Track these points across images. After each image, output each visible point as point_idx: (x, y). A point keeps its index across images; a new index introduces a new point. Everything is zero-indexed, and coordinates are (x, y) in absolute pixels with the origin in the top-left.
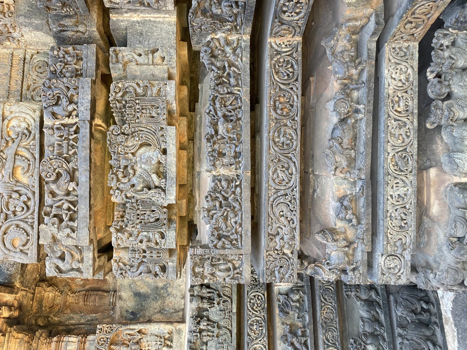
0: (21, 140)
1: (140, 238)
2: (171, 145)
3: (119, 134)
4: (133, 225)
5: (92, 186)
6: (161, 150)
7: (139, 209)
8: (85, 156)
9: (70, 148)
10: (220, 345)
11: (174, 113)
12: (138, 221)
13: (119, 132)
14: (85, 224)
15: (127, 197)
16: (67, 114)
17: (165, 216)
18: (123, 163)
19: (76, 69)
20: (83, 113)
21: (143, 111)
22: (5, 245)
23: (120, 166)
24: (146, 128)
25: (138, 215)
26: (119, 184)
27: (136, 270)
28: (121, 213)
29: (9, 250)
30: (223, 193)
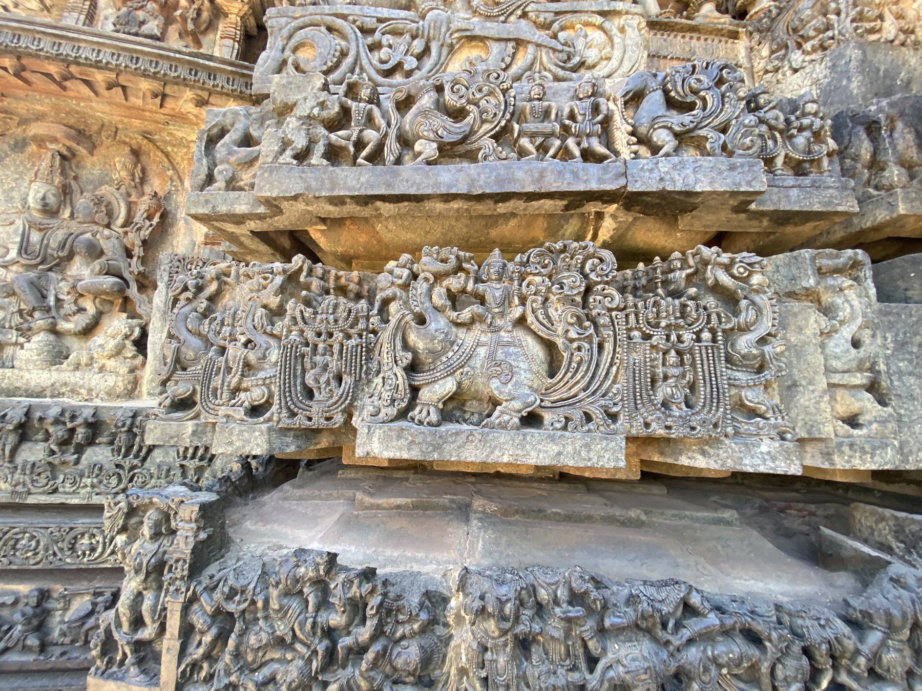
0: (554, 50)
1: (260, 339)
2: (556, 449)
3: (586, 276)
4: (299, 319)
5: (428, 205)
6: (539, 411)
7: (349, 337)
8: (512, 180)
9: (539, 140)
10: (164, 472)
11: (662, 454)
12: (310, 335)
13: (593, 276)
14: (313, 184)
15: (386, 302)
16: (643, 130)
17: (318, 422)
18: (493, 291)
19: (774, 158)
20: (651, 170)
21: (673, 353)
22: (302, 28)
23: (483, 282)
24: (611, 365)
25: (331, 335)
26: (426, 279)
27: (190, 327)
28: (352, 286)
29: (290, 37)
30: (377, 647)
